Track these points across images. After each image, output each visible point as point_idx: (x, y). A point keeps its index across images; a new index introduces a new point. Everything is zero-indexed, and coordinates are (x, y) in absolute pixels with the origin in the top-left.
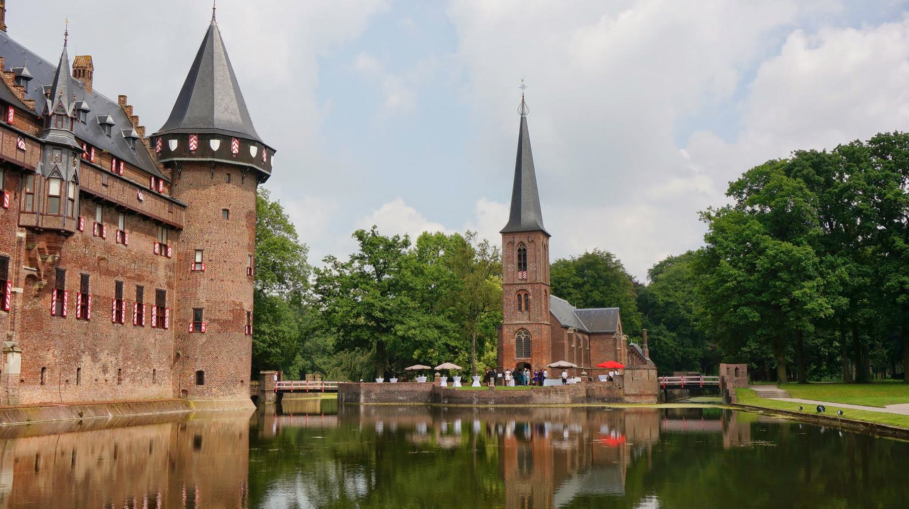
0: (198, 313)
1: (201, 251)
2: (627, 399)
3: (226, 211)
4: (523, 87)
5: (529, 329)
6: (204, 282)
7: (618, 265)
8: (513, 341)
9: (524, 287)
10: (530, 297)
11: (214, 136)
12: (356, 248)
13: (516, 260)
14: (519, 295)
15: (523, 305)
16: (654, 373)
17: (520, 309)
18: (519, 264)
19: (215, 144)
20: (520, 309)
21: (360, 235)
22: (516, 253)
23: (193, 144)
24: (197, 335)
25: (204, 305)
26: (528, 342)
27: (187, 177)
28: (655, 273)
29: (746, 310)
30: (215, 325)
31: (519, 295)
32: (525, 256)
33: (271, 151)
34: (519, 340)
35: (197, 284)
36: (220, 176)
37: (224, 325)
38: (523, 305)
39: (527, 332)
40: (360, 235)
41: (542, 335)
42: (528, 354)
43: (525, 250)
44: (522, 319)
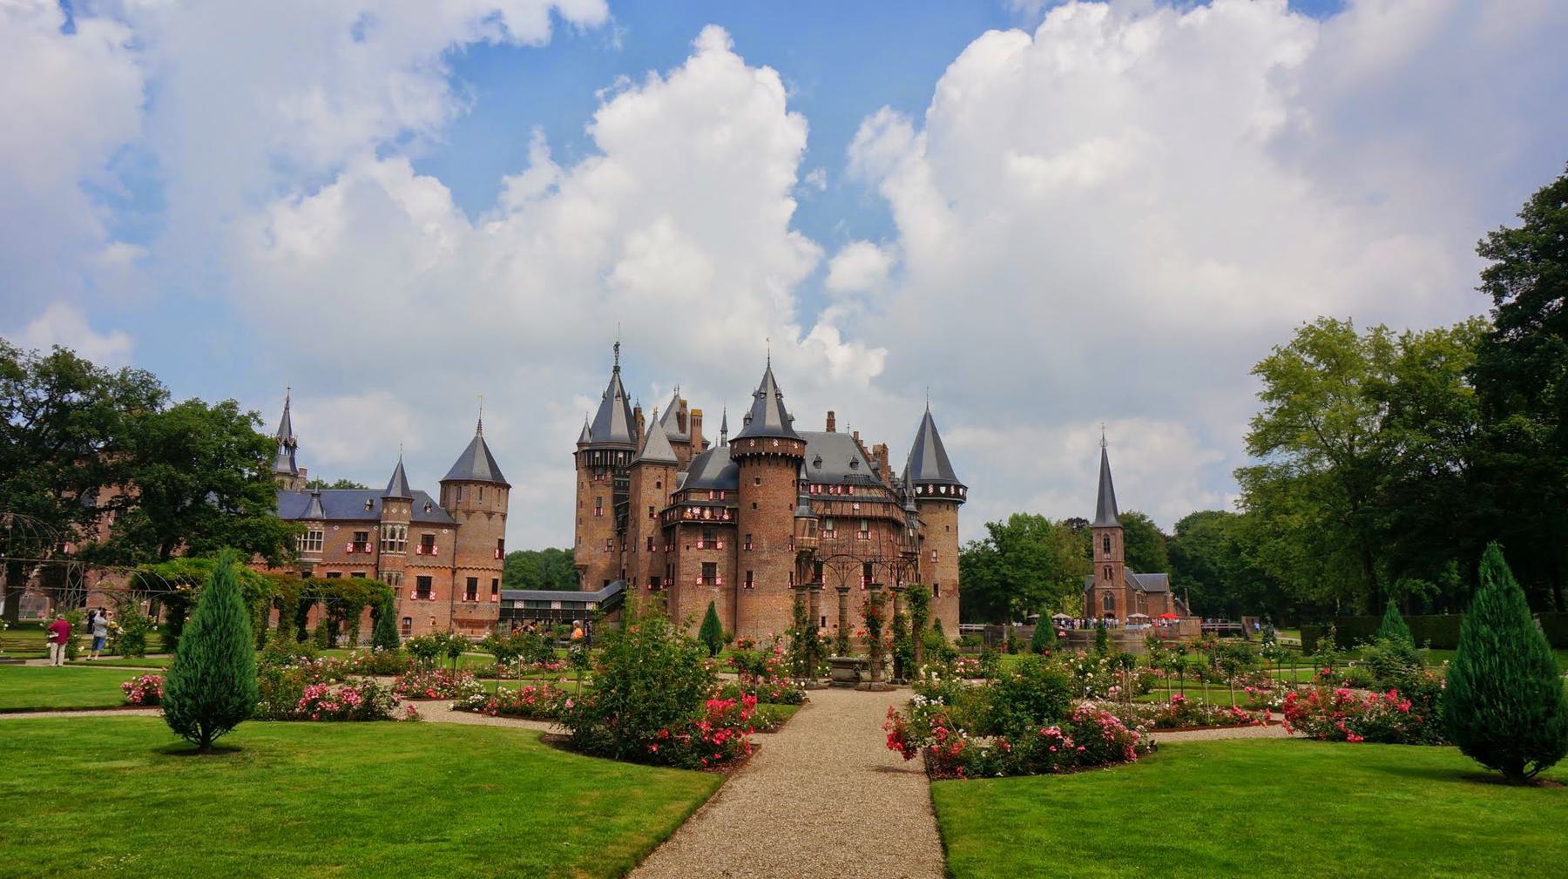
0: (936, 587)
1: (936, 551)
2: (1182, 637)
3: (947, 527)
4: (1103, 428)
5: (1112, 591)
6: (938, 568)
7: (1151, 525)
8: (1102, 599)
9: (1109, 564)
10: (1113, 571)
11: (943, 485)
12: (987, 534)
13: (1103, 546)
14: (1105, 570)
15: (1108, 576)
16: (1199, 621)
17: (1106, 578)
18: (1105, 549)
19: (943, 490)
20: (1106, 578)
21: (990, 526)
22: (1102, 542)
23: (931, 490)
24: (936, 599)
25: (939, 581)
26: (1112, 600)
27: (925, 508)
28: (1182, 527)
29: (1258, 584)
30: (945, 593)
31: (1105, 570)
32: (1108, 543)
33: (965, 488)
34: (1106, 599)
35: (934, 571)
36: (944, 507)
37: (949, 592)
38: (1108, 576)
39: (1111, 594)
40: (990, 526)
41: (1121, 595)
42: (1113, 607)
43: (1108, 539)
44: (1107, 585)
